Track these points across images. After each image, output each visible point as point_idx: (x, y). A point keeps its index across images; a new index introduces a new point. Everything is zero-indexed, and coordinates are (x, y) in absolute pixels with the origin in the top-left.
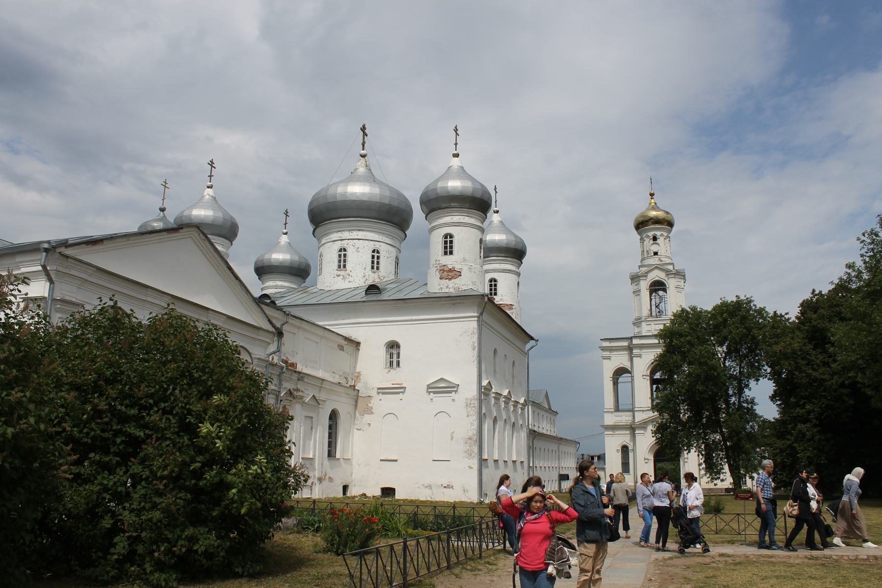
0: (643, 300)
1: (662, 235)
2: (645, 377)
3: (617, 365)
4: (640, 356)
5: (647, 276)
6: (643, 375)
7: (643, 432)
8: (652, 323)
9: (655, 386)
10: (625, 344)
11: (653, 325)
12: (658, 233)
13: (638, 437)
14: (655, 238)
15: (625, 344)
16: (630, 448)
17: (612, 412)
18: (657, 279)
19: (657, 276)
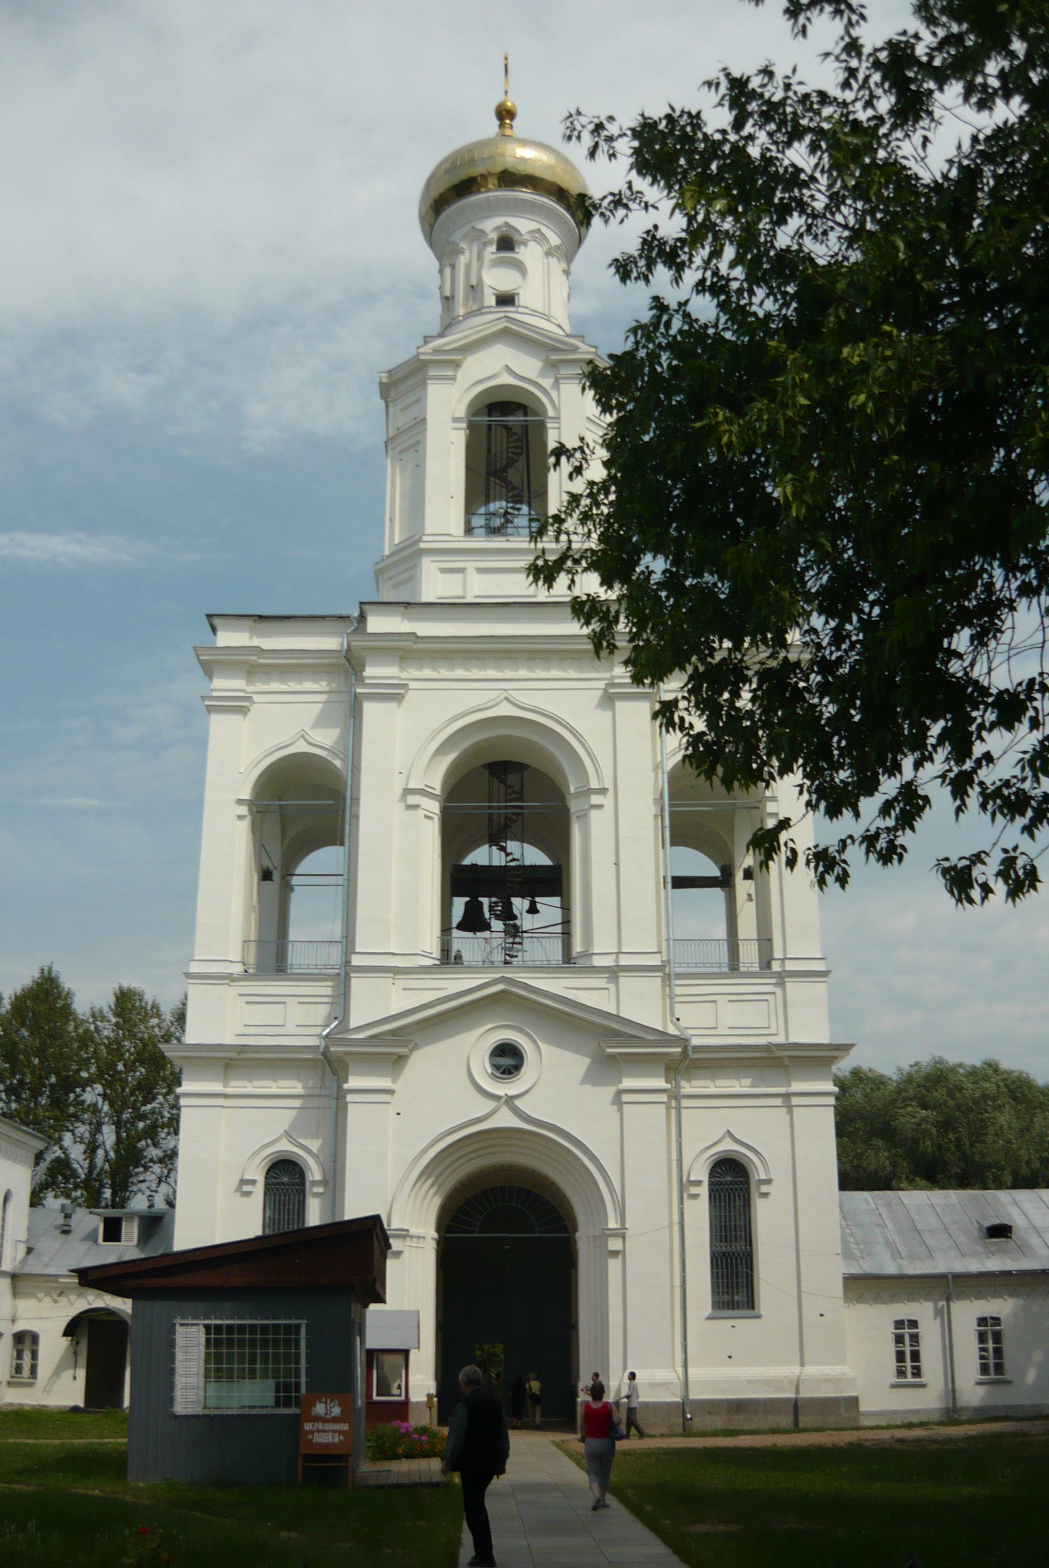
0: (432, 468)
1: (538, 236)
2: (412, 800)
3: (284, 739)
4: (394, 694)
5: (457, 365)
6: (407, 792)
7: (384, 1083)
8: (470, 565)
9: (459, 904)
10: (330, 642)
11: (471, 574)
12: (523, 225)
13: (357, 1114)
14: (506, 243)
15: (330, 642)
16: (314, 1173)
17: (230, 978)
18: (506, 379)
19: (508, 369)
